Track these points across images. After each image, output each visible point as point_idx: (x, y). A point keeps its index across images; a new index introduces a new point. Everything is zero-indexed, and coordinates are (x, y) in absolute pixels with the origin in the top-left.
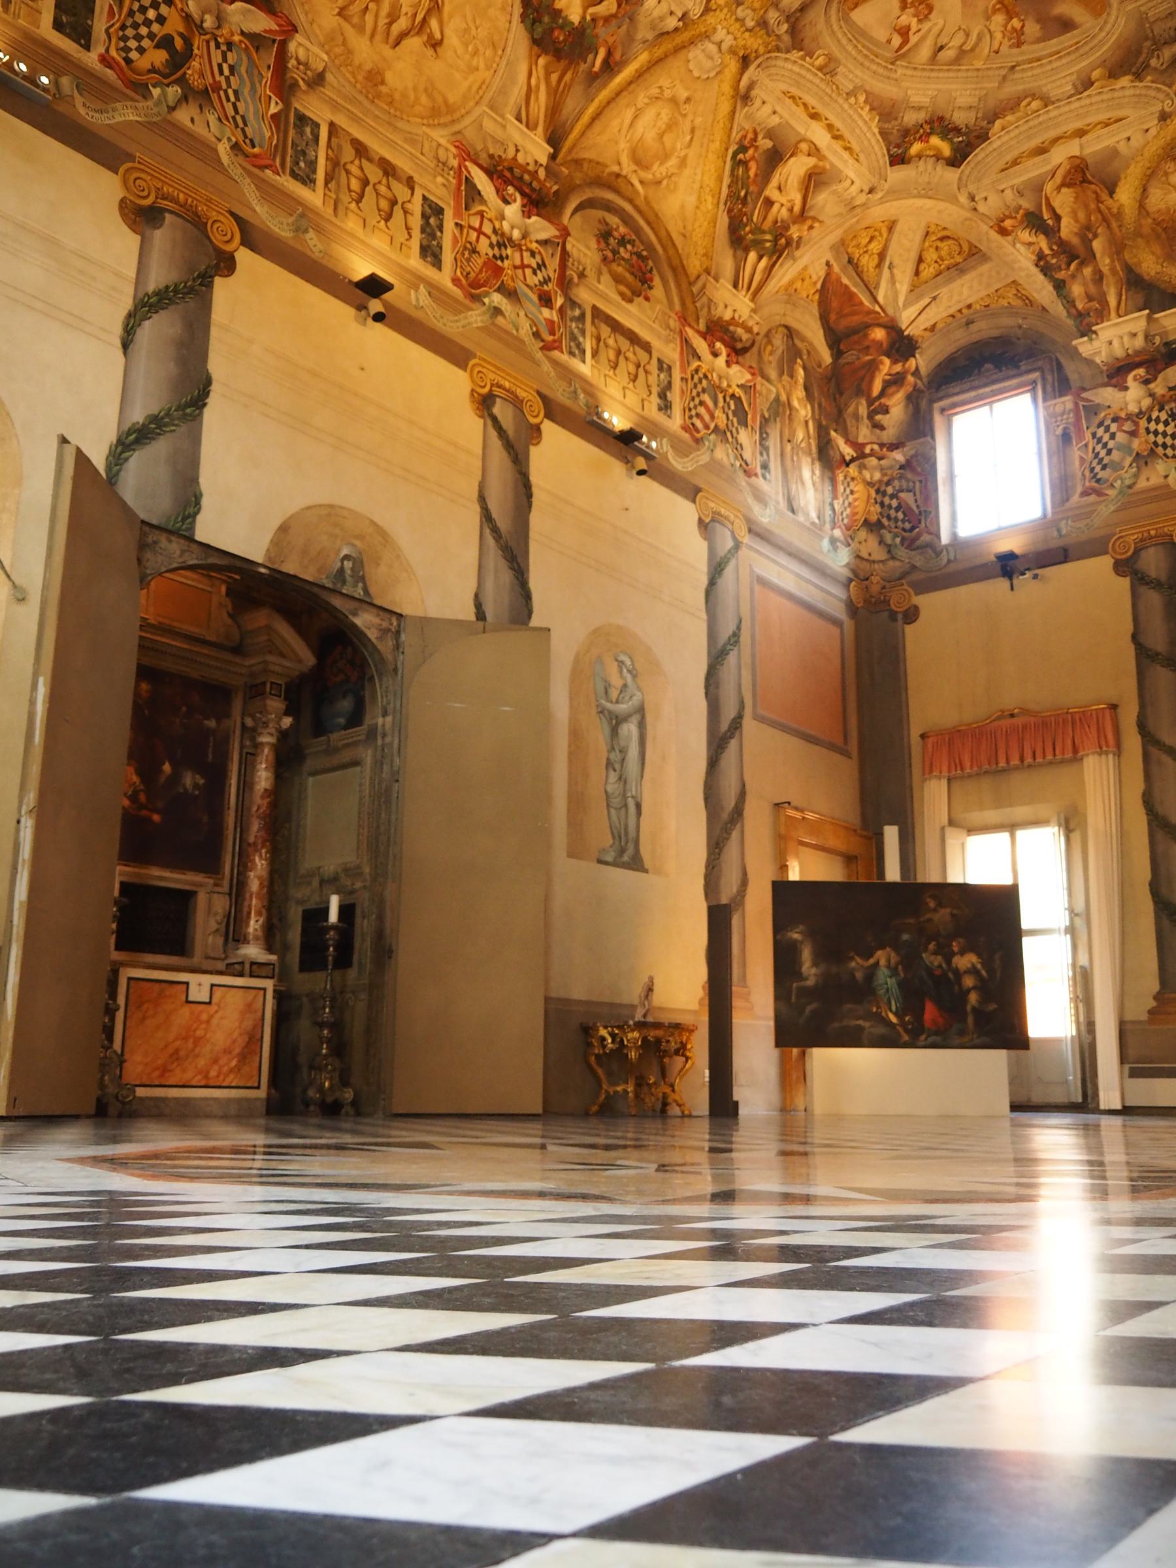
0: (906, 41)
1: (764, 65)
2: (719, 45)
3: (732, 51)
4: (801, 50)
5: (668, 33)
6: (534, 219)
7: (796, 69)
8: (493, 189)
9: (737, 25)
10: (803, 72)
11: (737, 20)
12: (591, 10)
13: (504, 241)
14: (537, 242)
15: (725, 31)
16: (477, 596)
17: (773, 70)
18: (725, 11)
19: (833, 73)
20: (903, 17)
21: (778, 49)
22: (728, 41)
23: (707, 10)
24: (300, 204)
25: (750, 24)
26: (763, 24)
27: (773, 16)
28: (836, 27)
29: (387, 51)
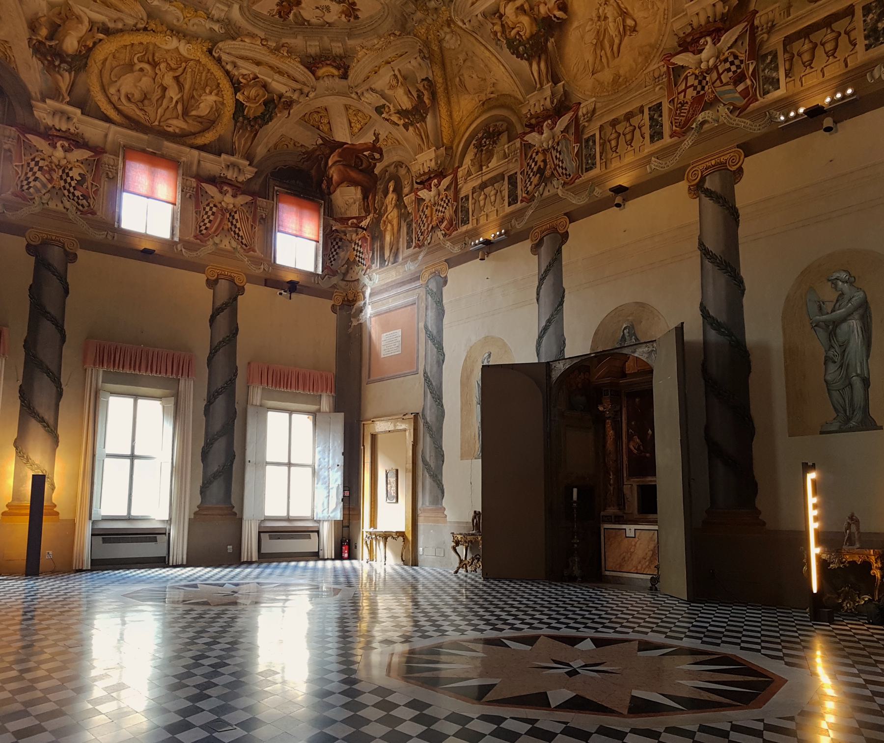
6: (722, 38)
8: (691, 55)
13: (701, 77)
14: (729, 48)
16: (701, 304)
24: (589, 181)
29: (617, 60)
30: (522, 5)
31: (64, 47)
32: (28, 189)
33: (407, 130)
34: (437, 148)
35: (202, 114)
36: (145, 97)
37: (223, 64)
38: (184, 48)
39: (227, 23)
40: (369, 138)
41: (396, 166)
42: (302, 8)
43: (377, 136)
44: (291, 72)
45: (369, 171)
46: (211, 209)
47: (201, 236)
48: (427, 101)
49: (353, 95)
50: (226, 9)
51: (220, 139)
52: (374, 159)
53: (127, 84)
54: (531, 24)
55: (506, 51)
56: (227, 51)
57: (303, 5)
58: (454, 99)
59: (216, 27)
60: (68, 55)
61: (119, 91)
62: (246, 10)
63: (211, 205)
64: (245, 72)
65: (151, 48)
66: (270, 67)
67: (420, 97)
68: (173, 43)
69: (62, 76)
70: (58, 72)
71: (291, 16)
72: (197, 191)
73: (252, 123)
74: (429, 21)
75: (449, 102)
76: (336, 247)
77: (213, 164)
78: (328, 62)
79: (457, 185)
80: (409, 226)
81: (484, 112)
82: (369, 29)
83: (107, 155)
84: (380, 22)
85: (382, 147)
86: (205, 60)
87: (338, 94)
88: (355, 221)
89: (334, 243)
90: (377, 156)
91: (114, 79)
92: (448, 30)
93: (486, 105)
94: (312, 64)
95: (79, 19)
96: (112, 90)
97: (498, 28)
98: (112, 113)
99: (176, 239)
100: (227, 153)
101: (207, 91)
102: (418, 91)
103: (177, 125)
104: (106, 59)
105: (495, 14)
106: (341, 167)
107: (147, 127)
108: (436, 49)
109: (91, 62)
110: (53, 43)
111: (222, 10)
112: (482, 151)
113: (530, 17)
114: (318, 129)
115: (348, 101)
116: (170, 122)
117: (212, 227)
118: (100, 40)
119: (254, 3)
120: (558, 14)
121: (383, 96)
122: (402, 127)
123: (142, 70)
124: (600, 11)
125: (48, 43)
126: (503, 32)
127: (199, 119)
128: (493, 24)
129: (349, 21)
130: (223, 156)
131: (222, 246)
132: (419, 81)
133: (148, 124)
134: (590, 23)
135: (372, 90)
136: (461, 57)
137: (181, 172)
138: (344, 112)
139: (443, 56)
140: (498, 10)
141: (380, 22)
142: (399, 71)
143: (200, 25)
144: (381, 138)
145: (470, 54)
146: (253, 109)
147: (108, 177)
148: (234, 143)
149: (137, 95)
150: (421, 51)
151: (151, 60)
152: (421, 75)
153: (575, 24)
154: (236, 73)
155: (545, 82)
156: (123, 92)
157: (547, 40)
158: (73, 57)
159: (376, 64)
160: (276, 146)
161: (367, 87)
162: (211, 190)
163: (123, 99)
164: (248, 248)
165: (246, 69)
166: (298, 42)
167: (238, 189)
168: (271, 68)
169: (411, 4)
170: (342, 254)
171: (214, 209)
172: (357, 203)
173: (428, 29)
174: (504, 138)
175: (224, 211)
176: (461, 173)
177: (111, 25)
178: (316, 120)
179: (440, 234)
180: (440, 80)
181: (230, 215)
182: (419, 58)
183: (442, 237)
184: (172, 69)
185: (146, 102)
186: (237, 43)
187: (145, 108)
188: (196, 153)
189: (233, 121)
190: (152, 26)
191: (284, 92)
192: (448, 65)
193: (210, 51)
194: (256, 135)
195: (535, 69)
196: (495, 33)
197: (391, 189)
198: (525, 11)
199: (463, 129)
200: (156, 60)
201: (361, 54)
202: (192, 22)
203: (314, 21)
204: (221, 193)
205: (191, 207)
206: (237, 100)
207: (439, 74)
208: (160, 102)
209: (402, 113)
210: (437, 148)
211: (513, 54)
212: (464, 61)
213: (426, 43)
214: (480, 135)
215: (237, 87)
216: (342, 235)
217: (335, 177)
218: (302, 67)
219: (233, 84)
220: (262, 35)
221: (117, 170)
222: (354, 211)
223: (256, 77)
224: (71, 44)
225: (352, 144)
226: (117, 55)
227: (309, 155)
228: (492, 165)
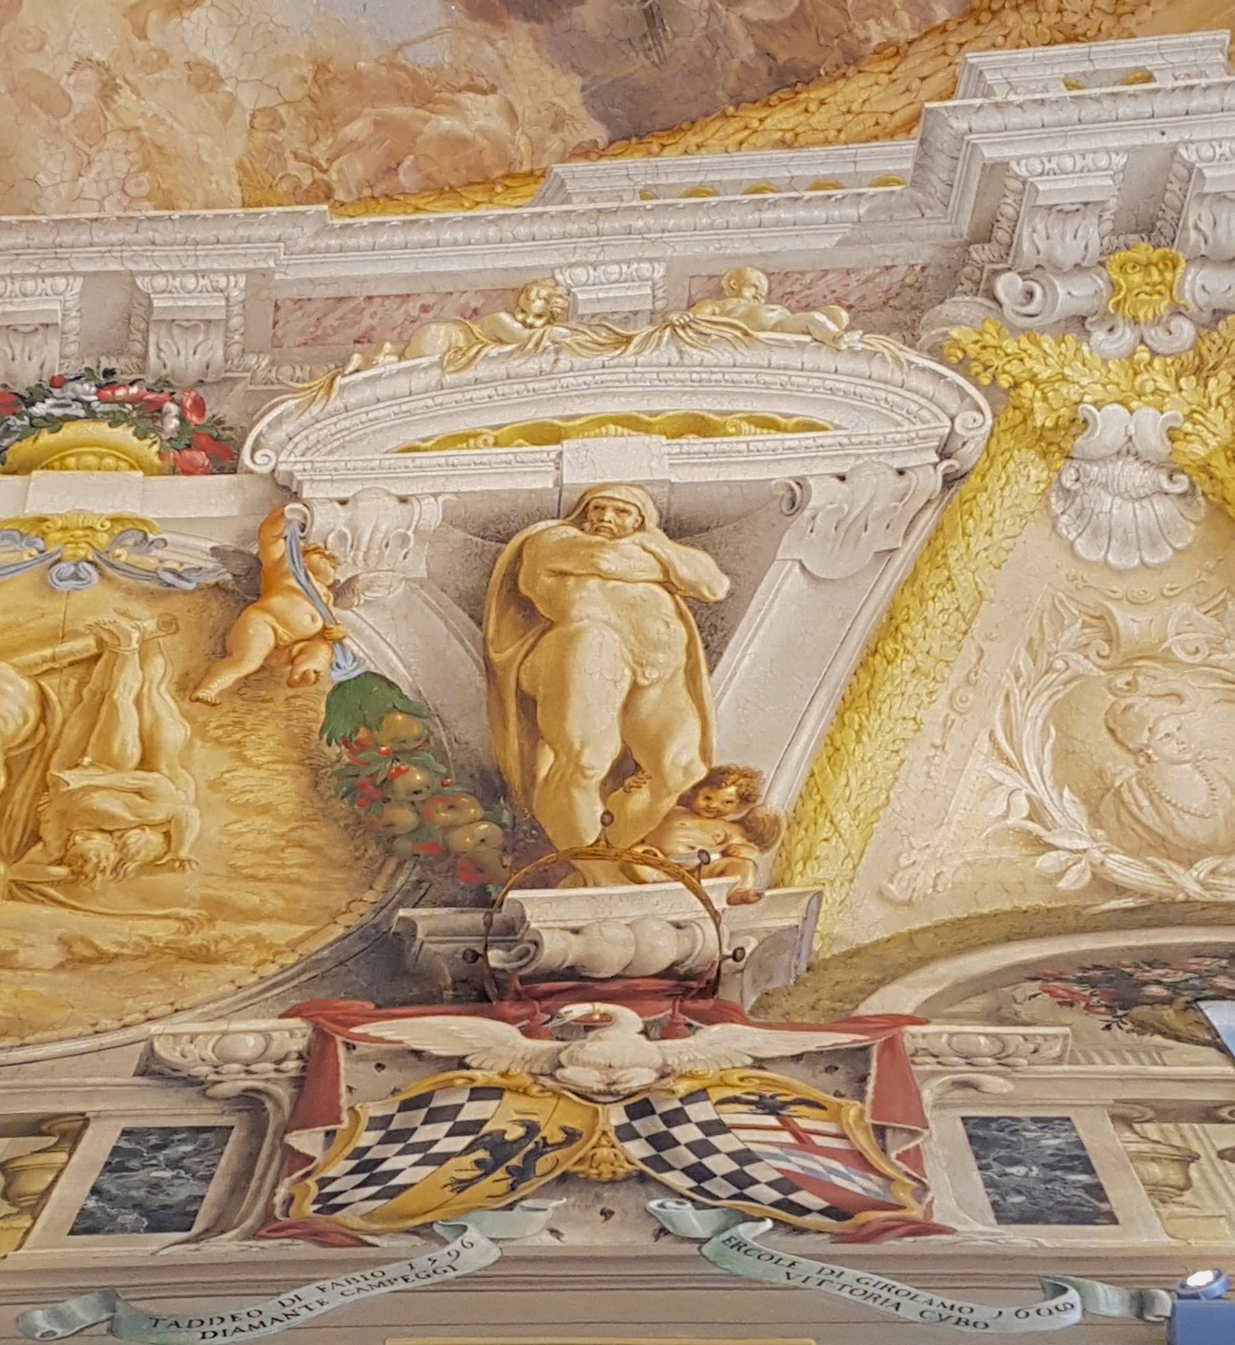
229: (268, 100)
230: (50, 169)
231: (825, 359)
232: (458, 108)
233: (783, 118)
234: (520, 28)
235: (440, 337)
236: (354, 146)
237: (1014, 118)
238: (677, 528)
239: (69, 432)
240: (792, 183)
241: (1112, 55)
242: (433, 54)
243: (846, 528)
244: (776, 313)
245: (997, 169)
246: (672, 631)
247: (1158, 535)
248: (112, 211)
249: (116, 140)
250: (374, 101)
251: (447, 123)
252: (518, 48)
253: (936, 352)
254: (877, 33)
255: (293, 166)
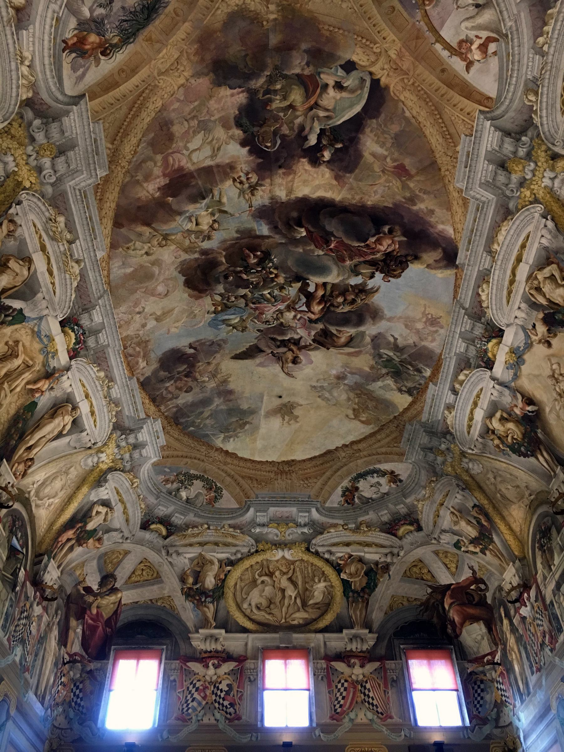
0: (489, 40)
1: (552, 140)
2: (552, 179)
3: (553, 169)
4: (531, 117)
5: (556, 225)
7: (544, 114)
9: (537, 173)
10: (544, 104)
11: (534, 175)
12: (559, 282)
15: (544, 180)
17: (553, 131)
18: (532, 187)
19: (535, 81)
20: (477, 57)
21: (538, 135)
22: (549, 174)
23: (536, 201)
25: (532, 164)
26: (529, 156)
27: (522, 152)
28: (508, 101)
30: (502, 416)
31: (206, 586)
32: (187, 710)
33: (485, 554)
34: (514, 563)
35: (318, 601)
36: (270, 602)
37: (322, 555)
38: (288, 554)
39: (312, 524)
40: (466, 574)
41: (499, 591)
42: (362, 491)
43: (471, 568)
44: (377, 541)
45: (482, 602)
46: (343, 685)
47: (337, 716)
48: (485, 524)
49: (433, 541)
50: (307, 514)
51: (338, 617)
52: (481, 590)
53: (255, 597)
54: (517, 426)
55: (514, 456)
56: (321, 544)
57: (361, 489)
58: (505, 513)
59: (306, 530)
60: (210, 591)
61: (250, 604)
62: (321, 509)
63: (343, 681)
64: (341, 555)
65: (265, 563)
66: (358, 543)
67: (479, 522)
68: (279, 554)
69: (208, 608)
70: (205, 606)
71: (356, 500)
72: (328, 672)
73: (361, 594)
74: (450, 460)
75: (503, 518)
76: (479, 691)
77: (337, 642)
78: (402, 522)
79: (541, 593)
80: (525, 648)
81: (533, 514)
82: (413, 485)
83: (249, 661)
84: (417, 476)
85: (482, 576)
86: (306, 557)
87: (422, 545)
88: (490, 657)
89: (476, 687)
90: (483, 586)
91: (245, 597)
92: (467, 460)
93: (532, 507)
94: (390, 528)
95: (212, 562)
96: (245, 606)
97: (497, 442)
98: (248, 625)
99: (314, 725)
100: (347, 628)
101: (317, 581)
102: (475, 518)
103: (300, 617)
104: (236, 584)
105: (488, 432)
106: (457, 607)
107: (277, 626)
108: (468, 478)
109: (226, 590)
110: (198, 586)
111: (305, 517)
112: (544, 551)
113: (513, 422)
114: (423, 579)
115: (434, 548)
116: (294, 616)
117: (345, 703)
118: (229, 571)
119: (324, 503)
120: (530, 408)
121: (454, 533)
122: (480, 554)
123: (263, 582)
124: (558, 389)
125: (195, 587)
126: (503, 442)
127: (317, 606)
128: (492, 440)
129: (397, 486)
130: (345, 631)
131: (358, 721)
132: (471, 509)
133: (277, 624)
134: (556, 403)
135: (444, 531)
136: (490, 476)
137: (311, 657)
138: (436, 558)
139: (476, 482)
140: (488, 429)
141: (417, 476)
142: (453, 507)
143: (292, 533)
144: (476, 568)
145: (495, 471)
146: (358, 582)
147: (250, 681)
148: (350, 617)
149: (264, 603)
150: (458, 485)
151: (267, 572)
152: (470, 505)
153: (547, 410)
154: (334, 558)
155: (555, 467)
156: (253, 604)
157: (536, 433)
158: (213, 591)
159: (434, 509)
160: (391, 607)
161: (438, 531)
162: (340, 666)
163: (255, 610)
164: (384, 716)
165: (340, 552)
166: (371, 516)
167: (366, 657)
168: (359, 544)
169: (430, 454)
170: (487, 697)
171: (346, 685)
172: (485, 638)
173: (452, 466)
174: (554, 531)
175: (354, 684)
176: (539, 578)
177: (233, 558)
178: (417, 572)
179: (547, 650)
180: (485, 502)
181: (362, 686)
182: (460, 491)
183: (549, 653)
184: (284, 574)
185: (272, 606)
186: (325, 535)
187: (273, 612)
188: (320, 636)
189: (345, 599)
190: (261, 547)
191: (378, 559)
192: (485, 488)
193: (308, 549)
194: (367, 603)
195: (542, 460)
196: (498, 446)
197: (503, 615)
198: (506, 419)
199: (526, 535)
200: (271, 570)
201: (420, 506)
202: (287, 533)
203: (374, 496)
204: (349, 666)
205: (324, 688)
206: (342, 580)
207: (482, 497)
208: (282, 602)
209: (474, 541)
210: (514, 563)
211: (520, 456)
212: (495, 478)
213: (458, 477)
214: (538, 537)
215: (338, 569)
216: (482, 677)
217: (457, 619)
218: (384, 534)
219: (335, 568)
220: (341, 522)
221: (257, 672)
222: (485, 647)
223: (350, 556)
224: (210, 582)
225: (457, 583)
226: (243, 577)
227: (426, 605)
228: (556, 562)
229: (141, 335)
230: (123, 309)
231: (107, 422)
232: (143, 361)
233: (147, 401)
234: (158, 365)
235: (102, 374)
236: (135, 349)
237: (150, 427)
238: (74, 422)
239: (73, 335)
240: (136, 406)
241: (161, 434)
242: (152, 355)
243: (79, 440)
244: (114, 413)
245: (142, 428)
246: (56, 432)
247: (86, 465)
248: (116, 320)
249: (130, 316)
250: (143, 350)
251: (140, 360)
252: (155, 365)
253: (111, 434)
254: (162, 408)
255: (129, 343)
